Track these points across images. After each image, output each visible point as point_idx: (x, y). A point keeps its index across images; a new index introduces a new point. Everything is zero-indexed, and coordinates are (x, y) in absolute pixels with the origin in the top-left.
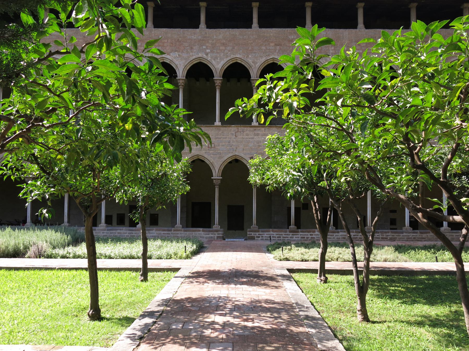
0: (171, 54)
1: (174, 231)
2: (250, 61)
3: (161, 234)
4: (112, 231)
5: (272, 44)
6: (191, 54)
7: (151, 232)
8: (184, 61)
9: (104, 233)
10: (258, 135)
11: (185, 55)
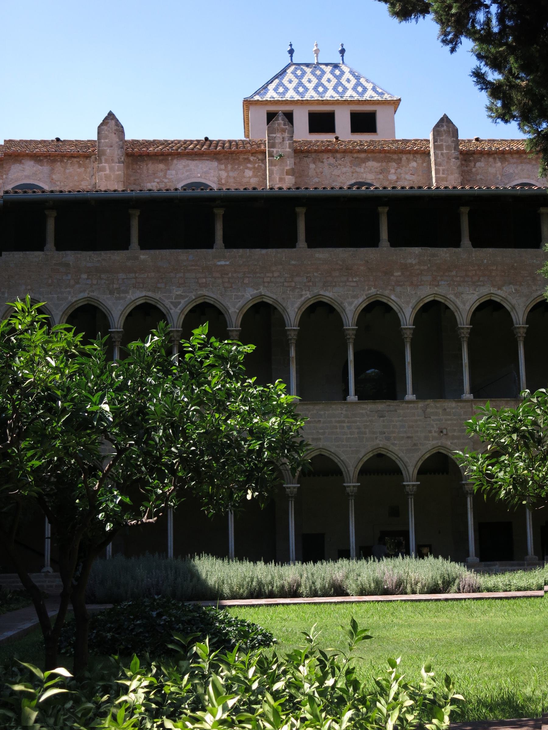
0: (504, 288)
6: (534, 288)
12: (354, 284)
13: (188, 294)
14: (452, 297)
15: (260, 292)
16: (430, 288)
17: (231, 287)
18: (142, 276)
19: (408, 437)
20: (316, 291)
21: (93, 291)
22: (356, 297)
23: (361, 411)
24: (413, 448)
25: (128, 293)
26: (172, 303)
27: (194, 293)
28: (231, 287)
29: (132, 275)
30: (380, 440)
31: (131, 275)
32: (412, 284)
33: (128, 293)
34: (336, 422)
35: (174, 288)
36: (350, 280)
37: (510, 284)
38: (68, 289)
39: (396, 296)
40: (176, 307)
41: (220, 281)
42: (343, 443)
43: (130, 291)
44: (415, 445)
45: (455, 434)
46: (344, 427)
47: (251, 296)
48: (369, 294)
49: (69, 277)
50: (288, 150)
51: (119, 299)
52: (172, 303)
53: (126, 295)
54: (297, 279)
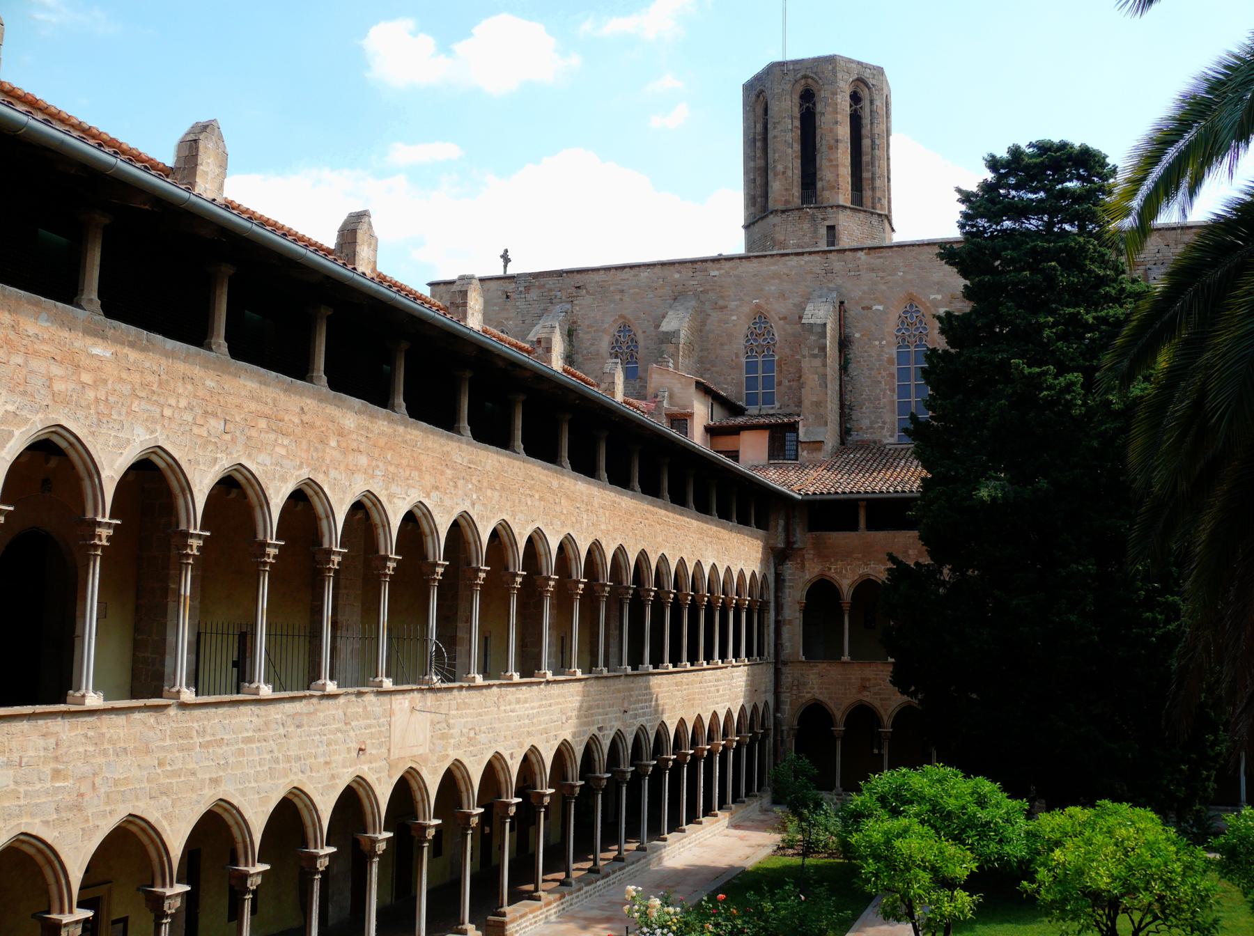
12: (283, 452)
14: (383, 499)
22: (284, 479)
41: (90, 394)
42: (250, 785)
48: (300, 476)
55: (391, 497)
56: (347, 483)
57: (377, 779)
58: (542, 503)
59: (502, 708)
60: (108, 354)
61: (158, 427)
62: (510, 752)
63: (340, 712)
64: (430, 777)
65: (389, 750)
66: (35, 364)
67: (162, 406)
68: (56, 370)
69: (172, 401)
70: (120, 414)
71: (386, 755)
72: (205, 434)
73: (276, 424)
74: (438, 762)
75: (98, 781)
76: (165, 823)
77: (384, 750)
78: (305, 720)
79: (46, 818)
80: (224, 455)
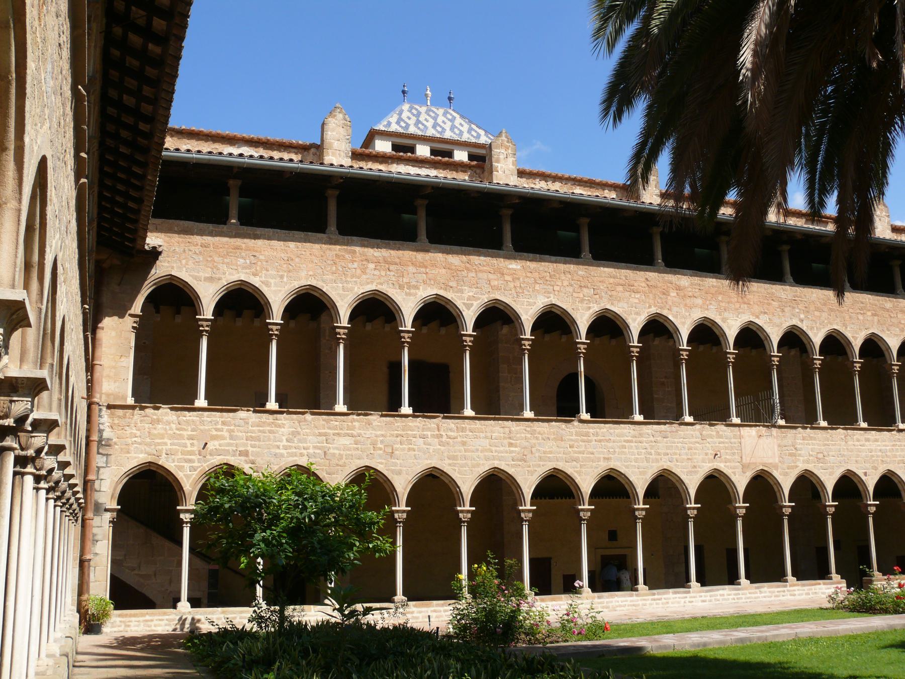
1: (791, 586)
2: (849, 335)
3: (774, 592)
4: (711, 593)
5: (869, 313)
7: (762, 590)
8: (777, 328)
9: (701, 596)
10: (868, 440)
11: (776, 320)
13: (480, 296)
15: (551, 301)
16: (701, 311)
17: (523, 293)
18: (433, 272)
19: (688, 459)
20: (602, 305)
21: (381, 284)
22: (638, 314)
23: (647, 431)
24: (693, 470)
25: (418, 289)
26: (464, 304)
27: (487, 296)
28: (523, 293)
29: (423, 270)
30: (665, 462)
31: (422, 270)
32: (686, 305)
33: (418, 289)
34: (625, 441)
35: (466, 288)
36: (633, 296)
37: (765, 313)
38: (354, 279)
39: (673, 317)
40: (468, 309)
43: (421, 287)
44: (695, 467)
45: (727, 457)
46: (632, 447)
47: (542, 303)
48: (650, 312)
49: (356, 265)
50: (511, 166)
51: (407, 294)
52: (464, 304)
53: (417, 291)
54: (585, 290)
55: (724, 320)
56: (687, 314)
57: (732, 472)
58: (876, 318)
59: (850, 443)
60: (519, 267)
61: (552, 295)
62: (864, 471)
63: (698, 433)
64: (781, 477)
65: (741, 458)
66: (480, 275)
67: (553, 286)
68: (491, 276)
69: (560, 283)
70: (529, 291)
71: (739, 460)
72: (582, 296)
73: (630, 287)
74: (788, 469)
75: (533, 450)
76: (576, 474)
77: (737, 457)
78: (669, 435)
79: (507, 463)
80: (595, 305)
